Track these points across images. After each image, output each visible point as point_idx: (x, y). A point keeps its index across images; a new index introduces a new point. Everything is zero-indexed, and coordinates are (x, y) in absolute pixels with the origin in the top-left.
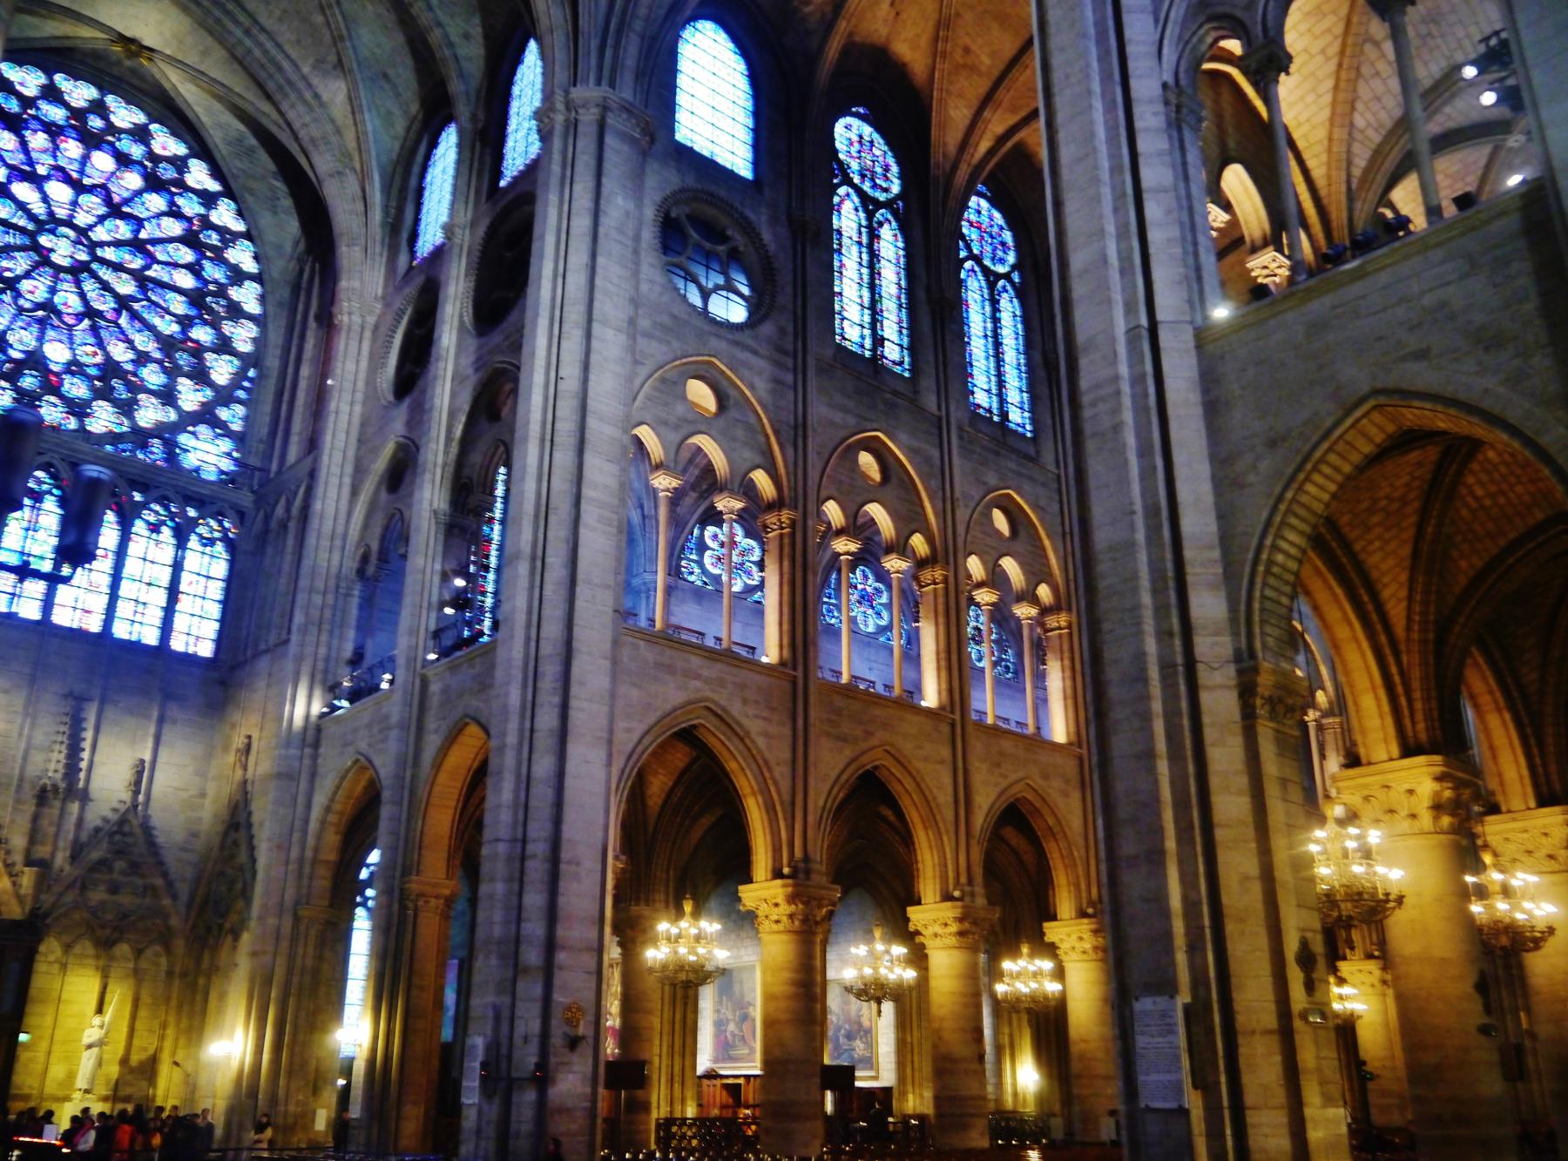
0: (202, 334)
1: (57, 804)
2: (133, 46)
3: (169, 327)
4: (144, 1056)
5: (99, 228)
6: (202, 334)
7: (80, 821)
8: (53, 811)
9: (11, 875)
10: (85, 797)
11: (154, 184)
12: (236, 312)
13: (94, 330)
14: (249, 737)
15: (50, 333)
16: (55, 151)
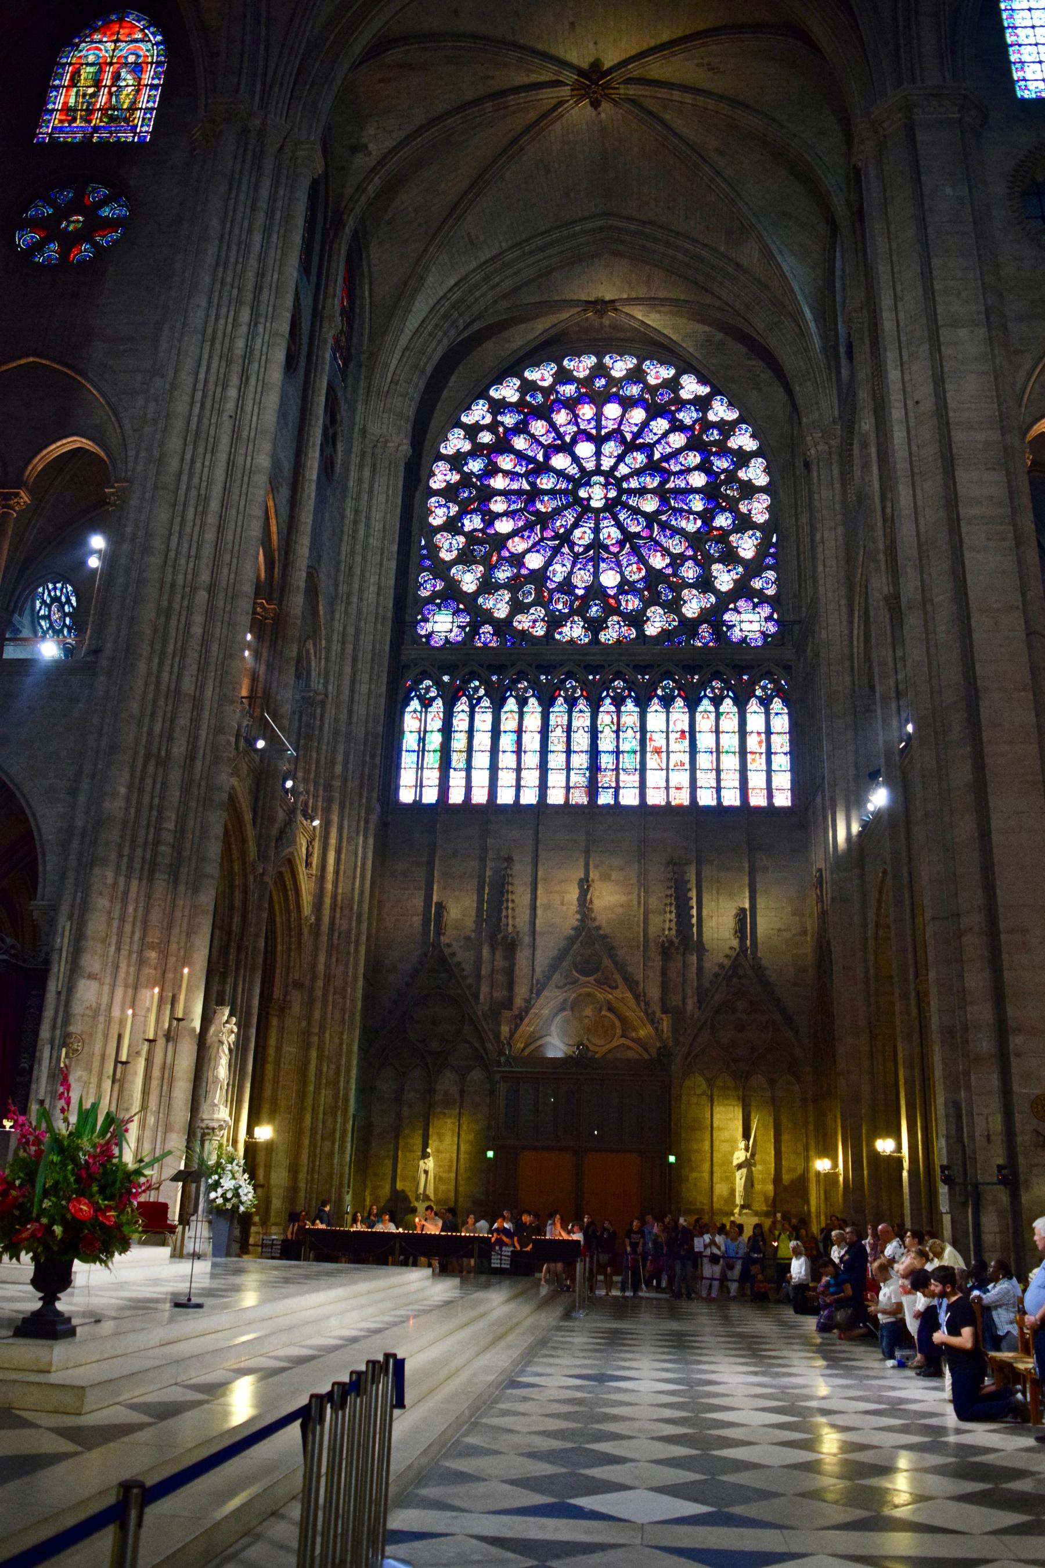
0: (723, 521)
1: (680, 957)
2: (601, 306)
3: (692, 526)
4: (793, 1176)
5: (622, 466)
6: (723, 521)
7: (700, 969)
8: (676, 965)
9: (652, 1022)
10: (700, 948)
11: (654, 412)
12: (749, 490)
13: (635, 551)
14: (820, 870)
15: (603, 565)
16: (575, 419)
